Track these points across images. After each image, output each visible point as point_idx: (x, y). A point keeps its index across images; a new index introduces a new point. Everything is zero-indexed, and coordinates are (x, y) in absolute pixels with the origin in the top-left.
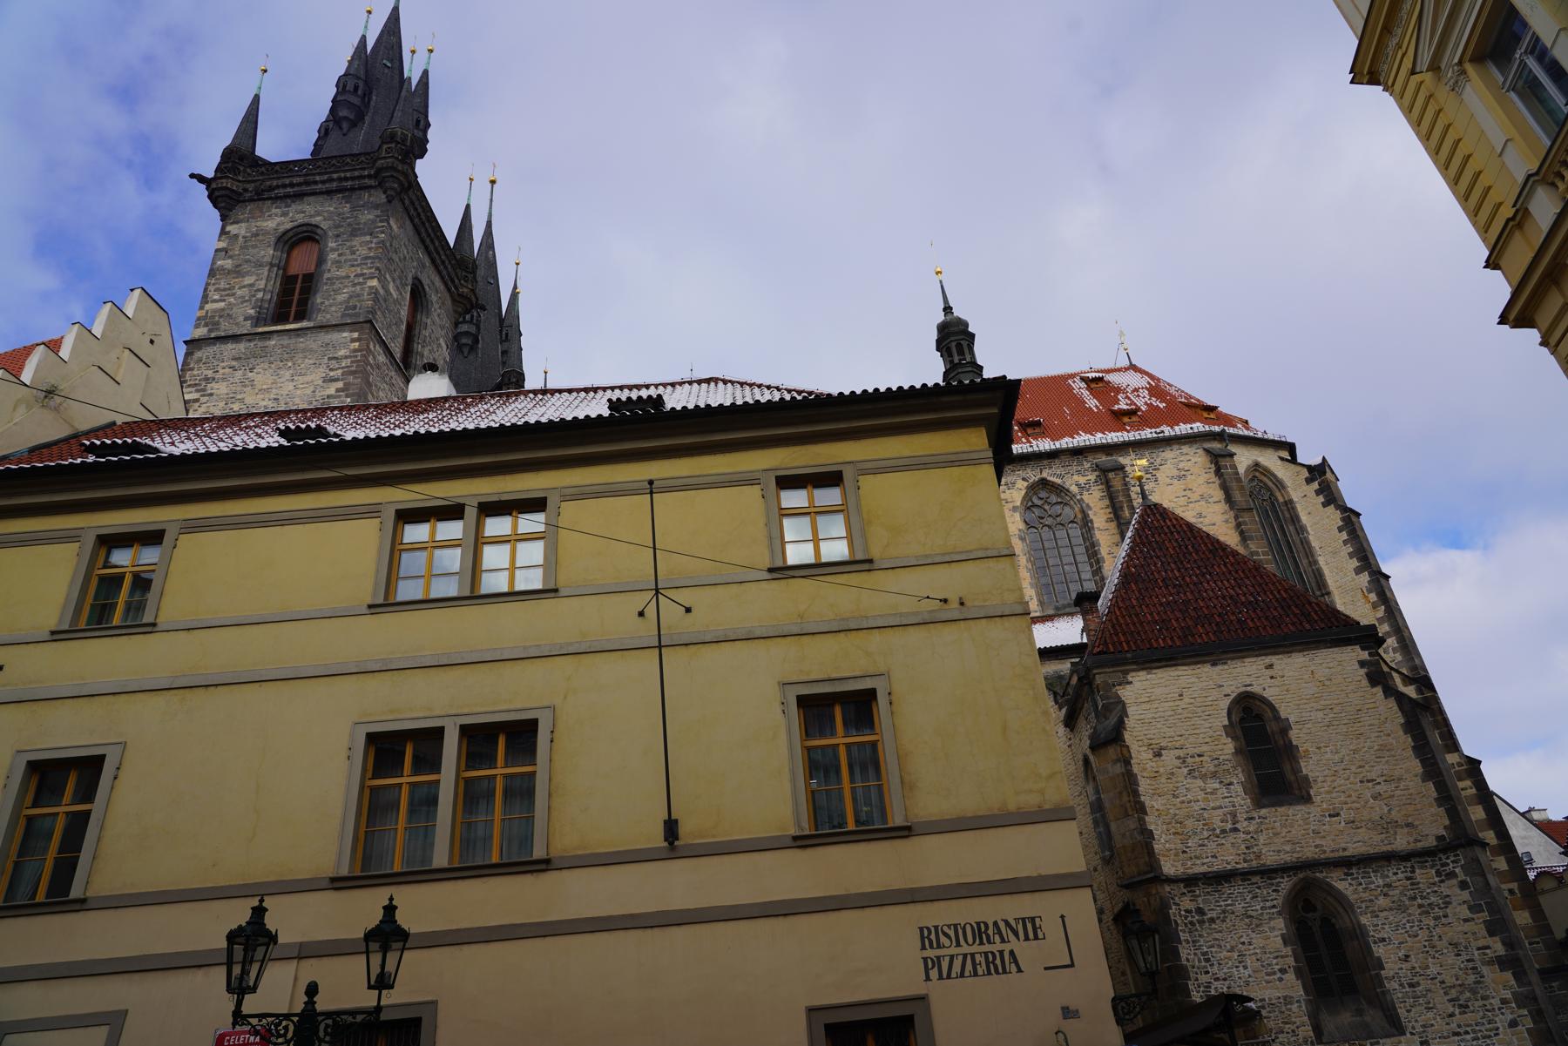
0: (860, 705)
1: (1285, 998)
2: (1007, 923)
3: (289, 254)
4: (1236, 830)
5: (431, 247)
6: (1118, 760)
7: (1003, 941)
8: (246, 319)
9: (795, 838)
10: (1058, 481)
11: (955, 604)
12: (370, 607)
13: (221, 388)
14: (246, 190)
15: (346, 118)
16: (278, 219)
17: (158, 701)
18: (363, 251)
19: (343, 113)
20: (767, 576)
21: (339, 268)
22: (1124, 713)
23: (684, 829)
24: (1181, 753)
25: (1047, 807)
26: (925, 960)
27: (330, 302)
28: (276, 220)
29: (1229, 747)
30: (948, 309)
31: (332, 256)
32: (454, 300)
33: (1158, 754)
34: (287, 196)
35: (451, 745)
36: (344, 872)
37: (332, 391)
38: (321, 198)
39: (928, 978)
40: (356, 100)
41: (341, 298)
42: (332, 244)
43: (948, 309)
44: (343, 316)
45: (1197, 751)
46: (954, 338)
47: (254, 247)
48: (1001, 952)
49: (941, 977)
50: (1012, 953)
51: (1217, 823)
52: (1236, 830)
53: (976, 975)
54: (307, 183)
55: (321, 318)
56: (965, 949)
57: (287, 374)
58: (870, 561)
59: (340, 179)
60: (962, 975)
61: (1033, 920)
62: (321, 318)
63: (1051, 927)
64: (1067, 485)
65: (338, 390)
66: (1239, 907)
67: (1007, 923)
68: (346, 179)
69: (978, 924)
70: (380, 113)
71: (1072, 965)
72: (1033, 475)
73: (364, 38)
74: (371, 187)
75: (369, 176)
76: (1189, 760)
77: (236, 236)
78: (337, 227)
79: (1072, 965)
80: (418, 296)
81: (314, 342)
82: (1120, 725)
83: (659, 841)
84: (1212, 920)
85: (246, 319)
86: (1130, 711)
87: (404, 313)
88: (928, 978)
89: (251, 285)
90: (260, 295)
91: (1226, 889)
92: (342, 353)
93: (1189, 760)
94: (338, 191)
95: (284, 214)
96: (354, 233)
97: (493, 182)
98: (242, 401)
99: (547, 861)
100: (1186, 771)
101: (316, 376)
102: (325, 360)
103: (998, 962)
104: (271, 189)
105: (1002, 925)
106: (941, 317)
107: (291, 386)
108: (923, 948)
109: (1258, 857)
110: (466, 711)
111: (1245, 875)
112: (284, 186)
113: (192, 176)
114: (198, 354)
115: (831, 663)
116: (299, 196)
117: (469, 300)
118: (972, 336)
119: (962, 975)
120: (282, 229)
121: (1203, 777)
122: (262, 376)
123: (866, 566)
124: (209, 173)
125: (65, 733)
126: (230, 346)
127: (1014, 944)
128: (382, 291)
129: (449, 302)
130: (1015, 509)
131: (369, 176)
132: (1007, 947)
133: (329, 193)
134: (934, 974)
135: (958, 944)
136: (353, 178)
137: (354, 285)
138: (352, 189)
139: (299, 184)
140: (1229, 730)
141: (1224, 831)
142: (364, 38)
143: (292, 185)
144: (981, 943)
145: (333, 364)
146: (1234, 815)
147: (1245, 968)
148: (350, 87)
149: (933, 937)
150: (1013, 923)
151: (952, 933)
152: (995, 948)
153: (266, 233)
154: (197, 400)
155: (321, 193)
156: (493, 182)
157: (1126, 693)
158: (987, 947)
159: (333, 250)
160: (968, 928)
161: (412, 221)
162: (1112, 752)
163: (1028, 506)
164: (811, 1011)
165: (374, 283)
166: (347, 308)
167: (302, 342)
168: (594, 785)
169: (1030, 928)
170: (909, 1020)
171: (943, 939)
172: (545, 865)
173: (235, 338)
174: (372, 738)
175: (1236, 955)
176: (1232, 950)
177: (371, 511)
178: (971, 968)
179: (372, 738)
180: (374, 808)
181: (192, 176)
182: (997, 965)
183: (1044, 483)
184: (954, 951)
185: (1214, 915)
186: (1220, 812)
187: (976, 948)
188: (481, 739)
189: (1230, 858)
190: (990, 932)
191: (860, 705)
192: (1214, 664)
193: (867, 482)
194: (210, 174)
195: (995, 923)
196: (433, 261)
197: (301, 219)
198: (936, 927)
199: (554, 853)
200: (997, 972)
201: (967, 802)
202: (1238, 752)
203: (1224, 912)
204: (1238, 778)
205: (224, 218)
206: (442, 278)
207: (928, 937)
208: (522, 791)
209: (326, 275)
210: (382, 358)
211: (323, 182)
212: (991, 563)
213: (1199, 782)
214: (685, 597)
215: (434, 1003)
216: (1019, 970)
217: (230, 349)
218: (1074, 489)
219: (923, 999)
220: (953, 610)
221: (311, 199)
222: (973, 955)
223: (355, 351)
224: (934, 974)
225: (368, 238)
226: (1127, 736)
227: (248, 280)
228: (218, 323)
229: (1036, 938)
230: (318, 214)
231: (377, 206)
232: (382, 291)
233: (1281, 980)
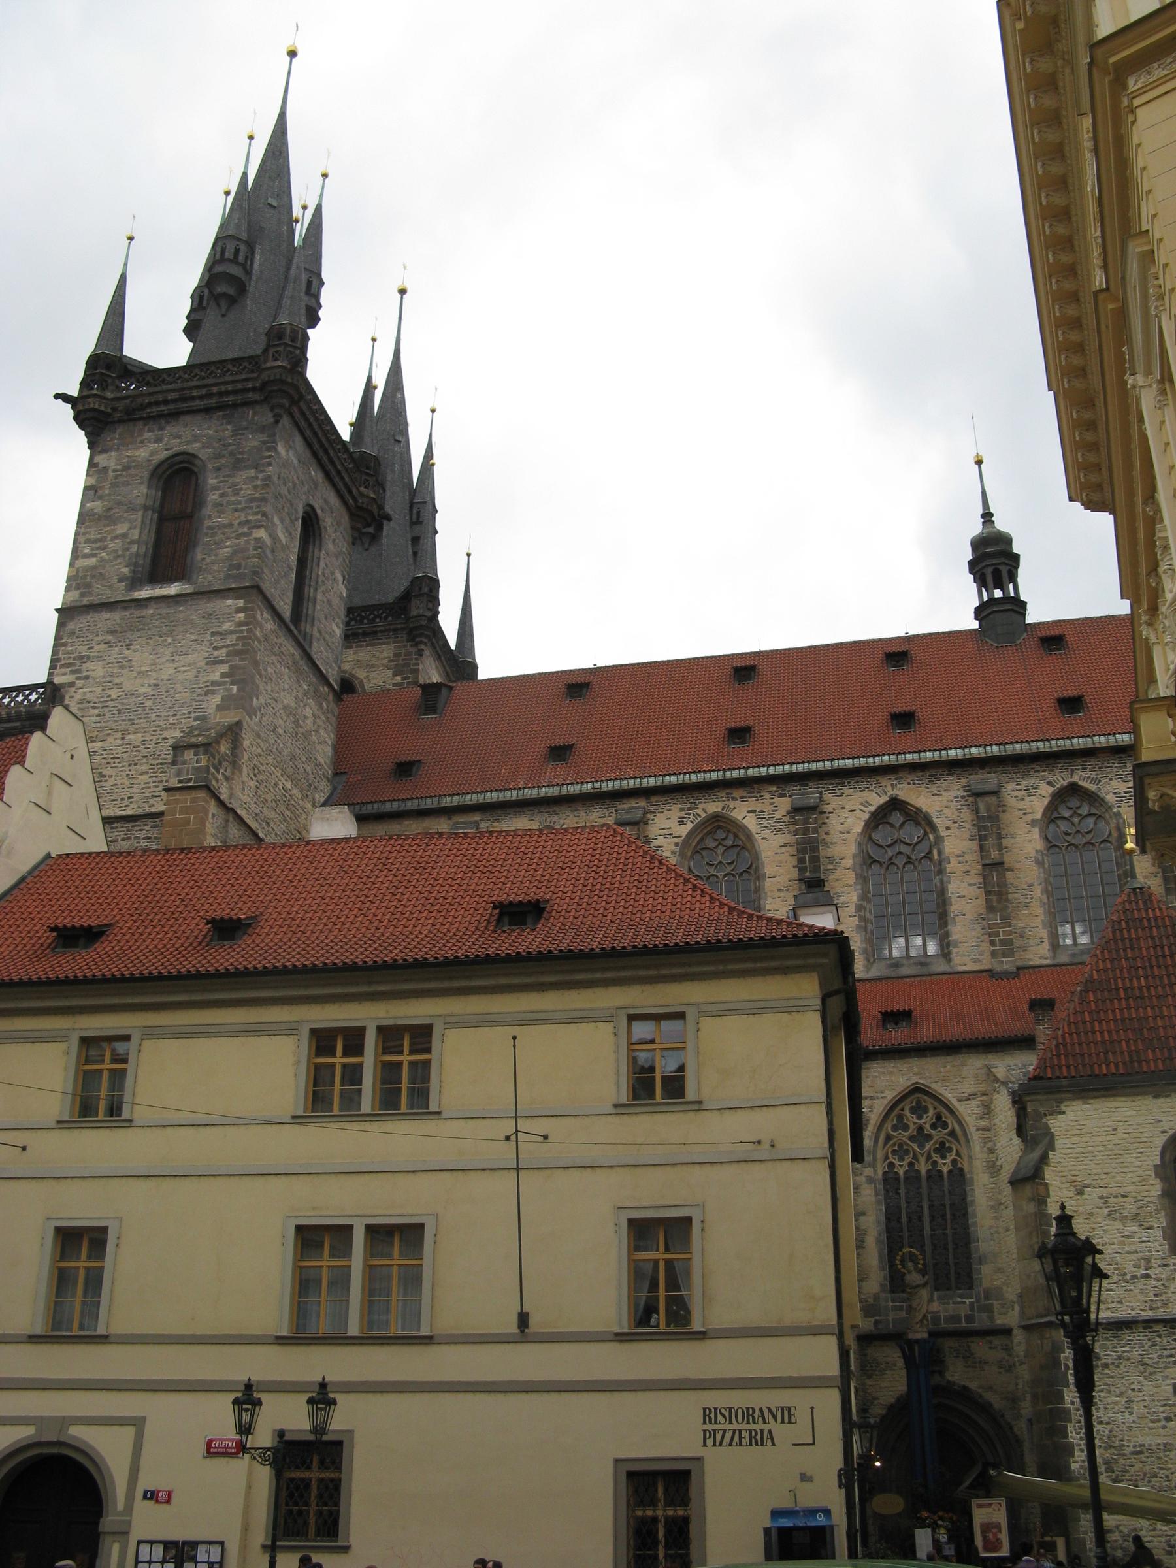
0: (677, 1229)
1: (1165, 1445)
2: (769, 1409)
3: (164, 491)
4: (1147, 1276)
5: (325, 459)
6: (1032, 1199)
7: (765, 1422)
8: (120, 581)
9: (617, 1334)
10: (1092, 787)
11: (766, 1146)
12: (293, 1117)
13: (96, 669)
14: (114, 409)
15: (225, 295)
16: (152, 447)
17: (144, 1185)
18: (247, 491)
19: (221, 289)
20: (613, 1111)
21: (221, 512)
22: (1051, 1146)
23: (532, 1321)
24: (1104, 1192)
25: (815, 1323)
26: (705, 1431)
27: (214, 557)
28: (150, 447)
29: (1156, 1188)
30: (987, 516)
31: (213, 497)
32: (352, 515)
33: (1080, 1193)
34: (160, 416)
35: (359, 1238)
36: (285, 1333)
37: (216, 676)
38: (198, 418)
39: (705, 1445)
40: (235, 270)
41: (225, 552)
42: (212, 481)
43: (987, 516)
44: (228, 576)
45: (1121, 1191)
46: (993, 559)
47: (127, 484)
48: (762, 1431)
49: (714, 1445)
50: (770, 1432)
51: (1129, 1267)
52: (1147, 1276)
53: (741, 1445)
54: (184, 399)
55: (204, 580)
56: (735, 1426)
57: (167, 653)
58: (700, 1102)
59: (221, 394)
60: (731, 1445)
61: (789, 1409)
62: (204, 580)
63: (802, 1415)
64: (1102, 794)
65: (223, 675)
66: (1136, 1355)
67: (769, 1409)
68: (227, 393)
69: (748, 1409)
70: (262, 266)
71: (813, 1444)
72: (1061, 778)
73: (245, 175)
74: (255, 402)
75: (254, 389)
76: (1112, 1200)
77: (105, 469)
78: (217, 457)
79: (813, 1444)
80: (310, 525)
81: (194, 612)
82: (1044, 1159)
83: (513, 1329)
84: (1106, 1366)
85: (120, 581)
86: (1059, 1143)
87: (293, 558)
88: (705, 1445)
89: (124, 536)
90: (134, 548)
91: (1126, 1335)
92: (227, 626)
93: (1112, 1200)
94: (220, 408)
95: (158, 440)
96: (238, 465)
97: (403, 292)
98: (119, 686)
99: (430, 1338)
100: (1106, 1211)
101: (199, 656)
102: (209, 637)
103: (758, 1438)
104: (143, 407)
105: (766, 1411)
106: (976, 528)
107: (170, 670)
108: (705, 1423)
109: (1165, 1304)
110: (369, 1212)
111: (1148, 1323)
112: (157, 403)
113: (57, 396)
114: (71, 626)
115: (657, 1194)
116: (175, 415)
117: (371, 513)
118: (1016, 558)
119: (731, 1445)
120: (156, 459)
121: (1123, 1219)
122: (140, 656)
123: (696, 1107)
124: (74, 392)
125: (81, 1207)
126: (106, 615)
127: (772, 1425)
128: (268, 541)
129: (345, 519)
130: (1034, 823)
131: (254, 389)
132: (766, 1427)
133: (207, 410)
134: (710, 1442)
135: (731, 1423)
136: (235, 392)
137: (238, 537)
138: (235, 406)
139: (174, 401)
140: (1161, 1171)
141: (1134, 1277)
142: (245, 175)
143: (166, 402)
144: (748, 1423)
145: (218, 642)
146: (1148, 1260)
147: (1131, 1414)
148: (229, 254)
149: (712, 1415)
150: (774, 1411)
151: (727, 1414)
152: (756, 1427)
153: (139, 466)
154: (72, 684)
155: (199, 411)
156: (403, 292)
157: (1057, 1124)
158: (752, 1426)
159: (215, 488)
160: (740, 1412)
161: (302, 433)
162: (1028, 1190)
163: (1051, 815)
164: (617, 1461)
165: (261, 533)
166: (231, 567)
167: (183, 612)
168: (465, 1282)
169: (787, 1414)
170: (687, 1473)
171: (720, 1418)
172: (428, 1340)
173: (109, 606)
174: (299, 1229)
175: (1123, 1400)
176: (1121, 1395)
177: (289, 1029)
178: (737, 1439)
179: (299, 1229)
180: (304, 1284)
181: (57, 396)
182: (756, 1439)
183: (1073, 789)
184: (727, 1427)
185: (1108, 1360)
186: (1134, 1256)
187: (744, 1426)
188: (379, 1234)
189: (1135, 1305)
190: (756, 1416)
191: (677, 1229)
192: (1156, 1097)
193: (707, 1024)
194: (74, 392)
195: (761, 1409)
196: (327, 475)
197: (177, 446)
198: (716, 1409)
199: (435, 1332)
200: (756, 1444)
201: (751, 1316)
202: (1166, 1194)
203: (1120, 1358)
204: (1160, 1221)
205: (92, 445)
206: (338, 491)
207: (709, 1415)
208: (413, 1279)
209: (207, 523)
210: (270, 625)
211: (201, 397)
212: (802, 1108)
213: (1118, 1225)
214: (540, 1126)
215: (351, 1432)
216: (773, 1444)
217: (106, 619)
218: (1111, 798)
219: (699, 1459)
220: (764, 1152)
221: (187, 418)
222: (740, 1431)
223: (240, 624)
224: (710, 1442)
225: (252, 472)
226: (1049, 1174)
227: (121, 529)
228: (89, 586)
229: (790, 1422)
230: (196, 439)
231: (263, 429)
232: (268, 541)
233: (1164, 1427)
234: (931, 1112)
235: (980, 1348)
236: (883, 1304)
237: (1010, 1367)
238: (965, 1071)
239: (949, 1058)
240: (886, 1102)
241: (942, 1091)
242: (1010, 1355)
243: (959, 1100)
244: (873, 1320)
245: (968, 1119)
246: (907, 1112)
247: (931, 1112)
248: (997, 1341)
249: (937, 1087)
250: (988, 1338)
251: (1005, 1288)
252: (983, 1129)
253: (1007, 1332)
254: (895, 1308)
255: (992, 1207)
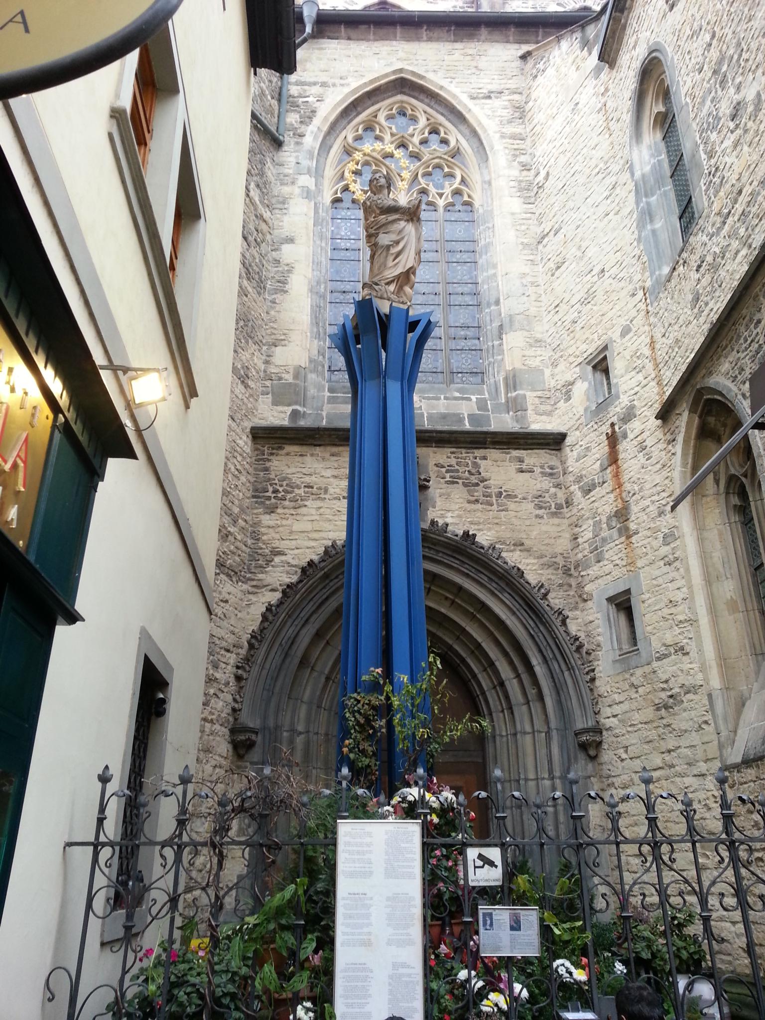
234: (423, 121)
235: (499, 469)
236: (312, 391)
237: (559, 507)
238: (483, 63)
239: (458, 45)
240: (346, 90)
241: (444, 83)
242: (558, 486)
243: (473, 98)
244: (289, 410)
245: (485, 121)
246: (381, 118)
247: (423, 121)
248: (534, 458)
249: (435, 80)
250: (515, 453)
251: (547, 372)
252: (514, 137)
253: (554, 442)
254: (332, 400)
255: (525, 245)
